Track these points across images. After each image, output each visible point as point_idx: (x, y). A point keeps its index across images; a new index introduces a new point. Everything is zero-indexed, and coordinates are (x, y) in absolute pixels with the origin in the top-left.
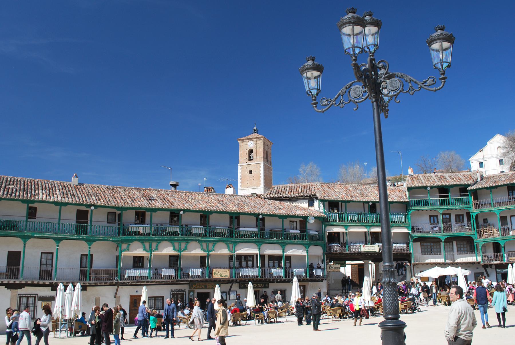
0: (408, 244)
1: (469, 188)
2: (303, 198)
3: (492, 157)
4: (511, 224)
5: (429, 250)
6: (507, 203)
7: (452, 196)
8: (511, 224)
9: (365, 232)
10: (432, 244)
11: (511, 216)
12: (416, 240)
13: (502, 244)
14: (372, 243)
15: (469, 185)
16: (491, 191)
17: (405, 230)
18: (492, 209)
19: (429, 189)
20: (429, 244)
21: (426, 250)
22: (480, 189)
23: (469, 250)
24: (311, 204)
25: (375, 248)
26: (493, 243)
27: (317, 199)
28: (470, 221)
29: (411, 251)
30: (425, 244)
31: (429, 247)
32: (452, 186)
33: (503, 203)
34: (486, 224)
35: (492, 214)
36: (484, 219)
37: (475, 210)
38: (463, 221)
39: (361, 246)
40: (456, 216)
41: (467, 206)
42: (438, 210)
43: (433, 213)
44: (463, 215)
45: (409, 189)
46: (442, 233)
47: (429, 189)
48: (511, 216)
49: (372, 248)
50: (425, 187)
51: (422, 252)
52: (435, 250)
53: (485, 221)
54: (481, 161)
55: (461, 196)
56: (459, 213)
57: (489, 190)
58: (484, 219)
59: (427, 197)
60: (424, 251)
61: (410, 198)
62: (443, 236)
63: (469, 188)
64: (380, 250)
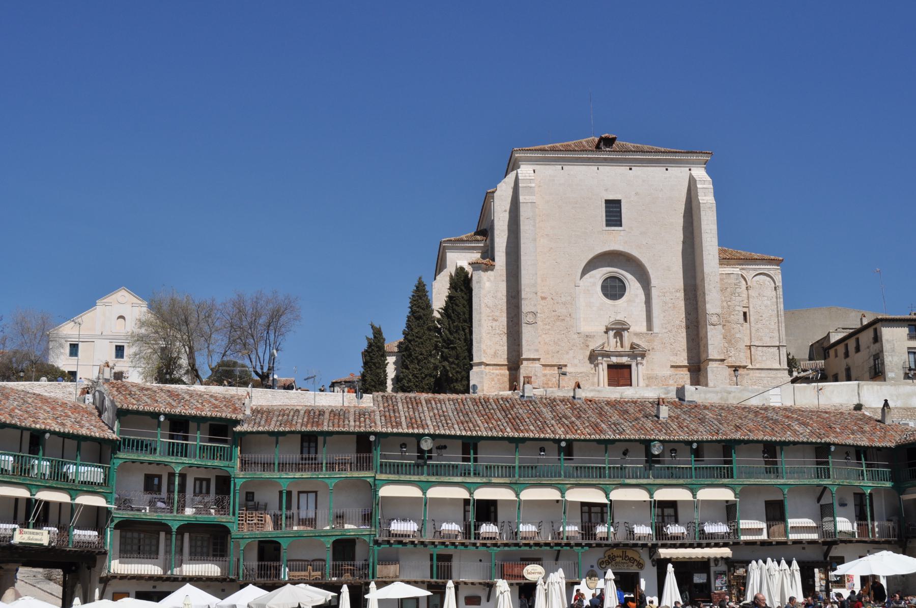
0: (102, 534)
1: (238, 428)
3: (102, 336)
4: (298, 508)
5: (136, 548)
6: (298, 467)
7: (197, 439)
8: (298, 508)
9: (17, 500)
10: (142, 536)
11: (299, 493)
12: (123, 525)
13: (284, 544)
14: (38, 525)
15: (237, 422)
16: (277, 443)
17: (98, 501)
18: (276, 475)
19: (162, 418)
20: (136, 535)
21: (129, 547)
22: (252, 433)
23: (211, 553)
25: (43, 537)
26: (260, 542)
28: (229, 494)
29: (108, 548)
30: (129, 535)
31: (136, 541)
32: (195, 418)
33: (291, 464)
34: (250, 503)
35: (270, 482)
36: (247, 493)
37: (241, 475)
38: (208, 492)
39: (14, 530)
40: (196, 479)
41: (226, 463)
42: (173, 465)
43: (153, 470)
44: (208, 481)
46: (175, 514)
47: (162, 418)
48: (299, 493)
49: (38, 537)
50: (155, 415)
51: (120, 551)
52: (147, 548)
53: (250, 496)
54: (74, 340)
55: (211, 440)
56: (202, 474)
57: (274, 438)
58: (247, 493)
59: (156, 435)
60: (127, 552)
61: (121, 432)
62: (174, 520)
63: (238, 428)
64: (50, 543)
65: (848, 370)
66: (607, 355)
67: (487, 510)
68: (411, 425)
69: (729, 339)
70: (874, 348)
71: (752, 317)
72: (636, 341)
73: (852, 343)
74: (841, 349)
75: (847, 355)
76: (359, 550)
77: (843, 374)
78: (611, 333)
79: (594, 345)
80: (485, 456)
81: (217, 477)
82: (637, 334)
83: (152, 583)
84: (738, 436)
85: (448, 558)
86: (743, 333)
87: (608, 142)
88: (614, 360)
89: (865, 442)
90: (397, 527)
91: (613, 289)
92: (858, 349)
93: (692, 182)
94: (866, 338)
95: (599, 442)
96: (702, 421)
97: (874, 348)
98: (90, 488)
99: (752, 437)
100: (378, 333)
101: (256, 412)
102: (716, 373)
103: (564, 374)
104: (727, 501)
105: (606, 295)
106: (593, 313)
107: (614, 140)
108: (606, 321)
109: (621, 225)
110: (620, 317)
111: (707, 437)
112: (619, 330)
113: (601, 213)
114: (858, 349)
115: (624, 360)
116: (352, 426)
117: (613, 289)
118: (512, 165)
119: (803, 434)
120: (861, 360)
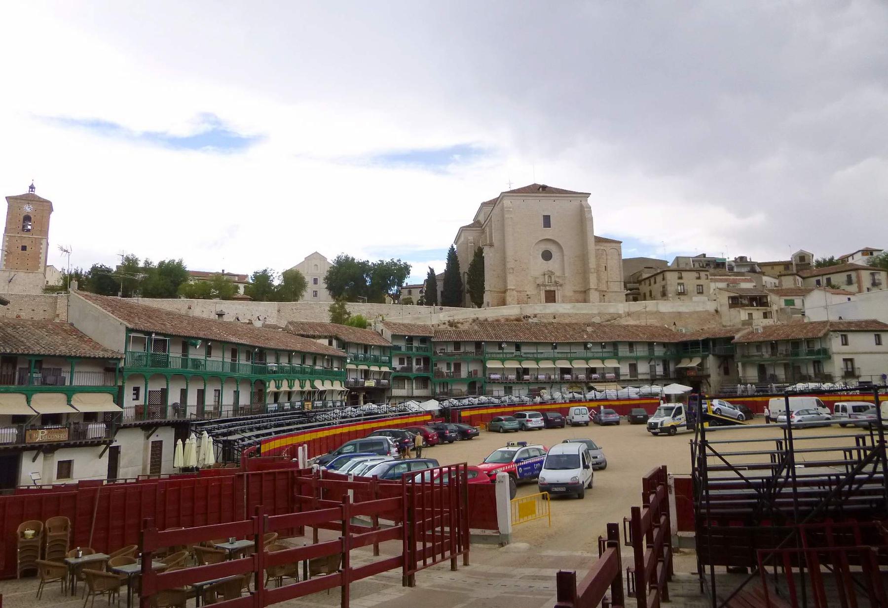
2: (325, 337)
24: (330, 343)
27: (337, 339)
45: (394, 337)
65: (651, 292)
66: (545, 286)
67: (526, 371)
68: (496, 338)
69: (599, 279)
70: (663, 283)
71: (609, 269)
73: (652, 281)
74: (647, 282)
75: (650, 285)
76: (477, 386)
77: (648, 294)
79: (540, 281)
80: (524, 350)
84: (619, 340)
85: (511, 388)
86: (604, 276)
88: (548, 288)
89: (667, 341)
90: (493, 376)
91: (547, 256)
92: (655, 283)
94: (659, 278)
95: (568, 343)
96: (605, 332)
97: (663, 283)
98: (384, 364)
99: (625, 340)
100: (432, 270)
101: (436, 332)
102: (594, 296)
106: (539, 266)
111: (608, 340)
112: (551, 274)
113: (541, 221)
115: (552, 289)
116: (476, 338)
119: (644, 338)
120: (657, 288)
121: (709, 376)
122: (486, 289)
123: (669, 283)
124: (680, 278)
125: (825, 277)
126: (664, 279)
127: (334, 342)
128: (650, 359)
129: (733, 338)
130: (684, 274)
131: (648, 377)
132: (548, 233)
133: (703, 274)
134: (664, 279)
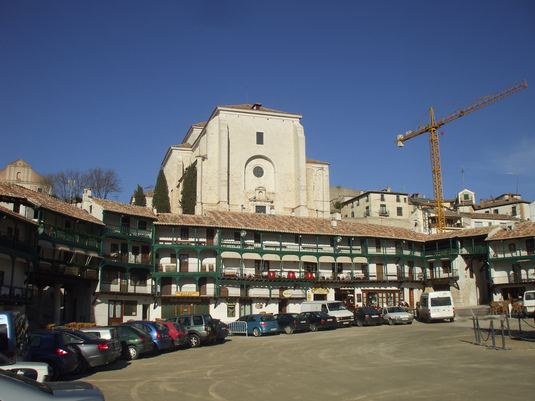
1: (155, 223)
45: (106, 213)
63: (155, 223)
70: (367, 204)
72: (268, 196)
75: (352, 207)
78: (258, 191)
79: (252, 196)
81: (142, 246)
82: (269, 193)
83: (115, 296)
87: (258, 107)
88: (259, 204)
91: (258, 172)
92: (358, 205)
93: (295, 127)
103: (244, 208)
104: (362, 264)
105: (255, 175)
107: (260, 106)
108: (256, 187)
109: (263, 144)
110: (262, 185)
112: (260, 190)
114: (358, 205)
115: (263, 204)
116: (207, 224)
117: (258, 172)
118: (215, 113)
121: (457, 278)
122: (198, 200)
123: (372, 204)
124: (382, 199)
125: (493, 209)
126: (367, 201)
127: (22, 208)
128: (396, 259)
129: (486, 236)
130: (385, 196)
131: (395, 278)
132: (260, 150)
133: (402, 197)
134: (367, 201)
